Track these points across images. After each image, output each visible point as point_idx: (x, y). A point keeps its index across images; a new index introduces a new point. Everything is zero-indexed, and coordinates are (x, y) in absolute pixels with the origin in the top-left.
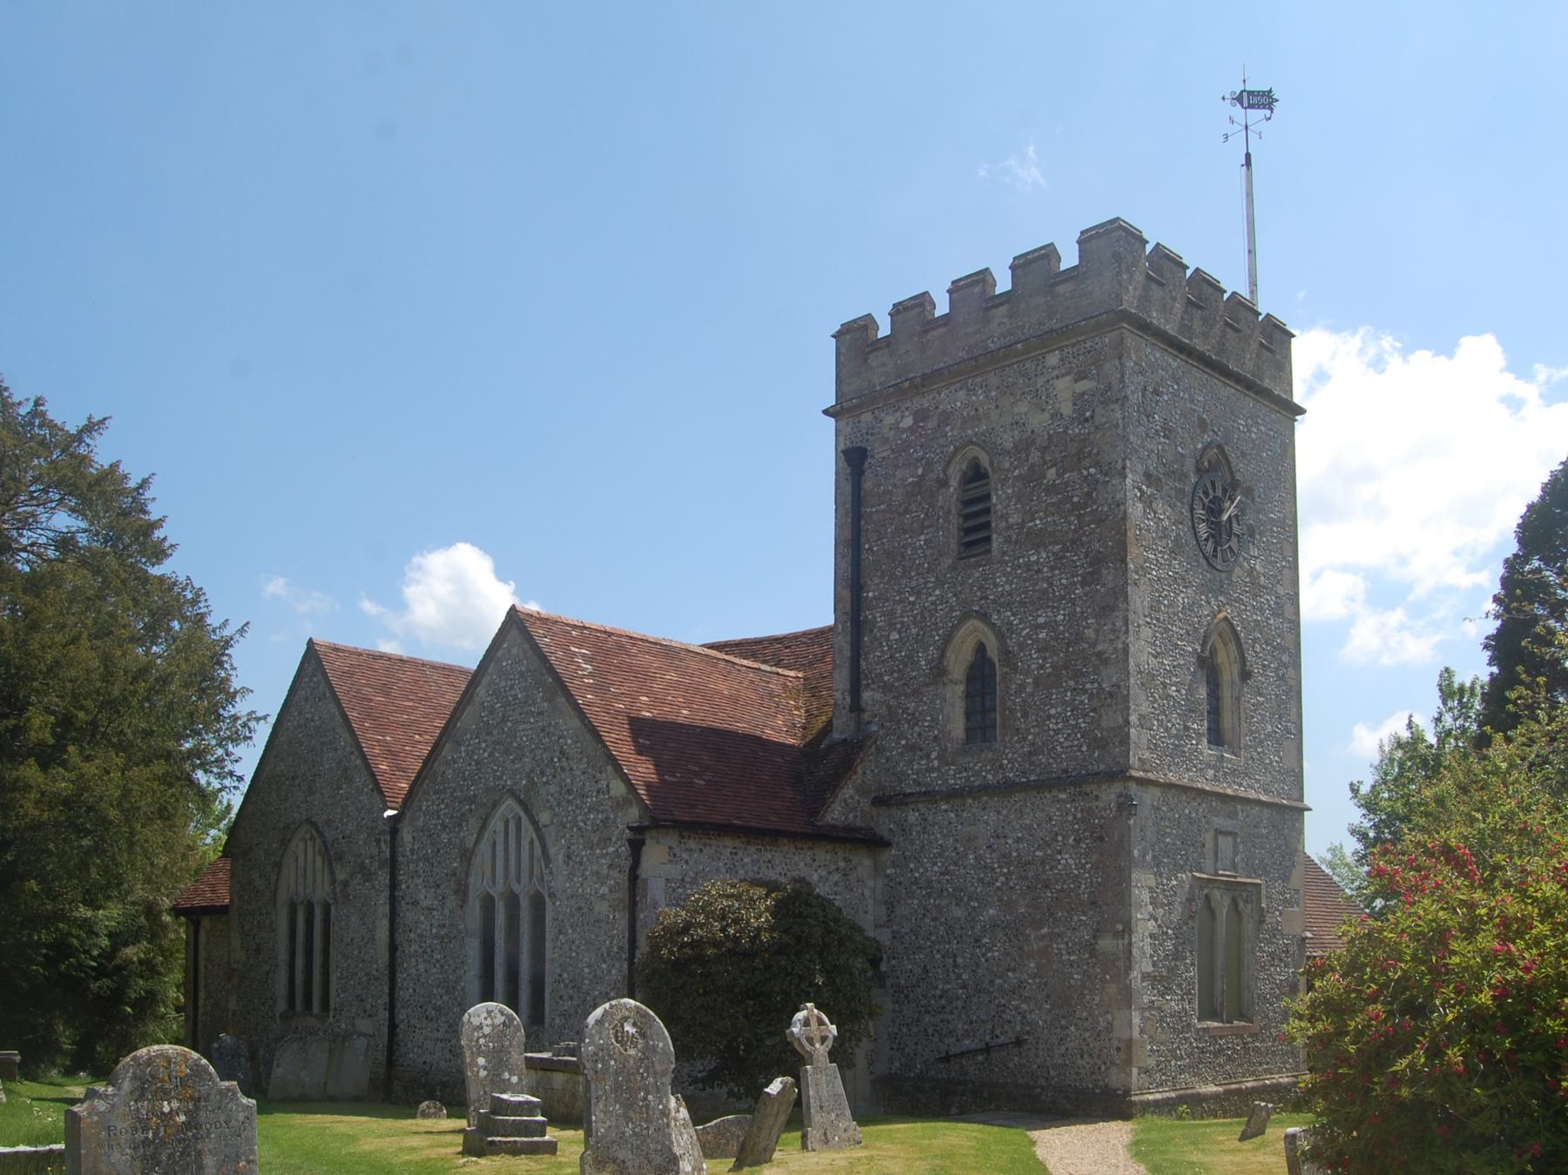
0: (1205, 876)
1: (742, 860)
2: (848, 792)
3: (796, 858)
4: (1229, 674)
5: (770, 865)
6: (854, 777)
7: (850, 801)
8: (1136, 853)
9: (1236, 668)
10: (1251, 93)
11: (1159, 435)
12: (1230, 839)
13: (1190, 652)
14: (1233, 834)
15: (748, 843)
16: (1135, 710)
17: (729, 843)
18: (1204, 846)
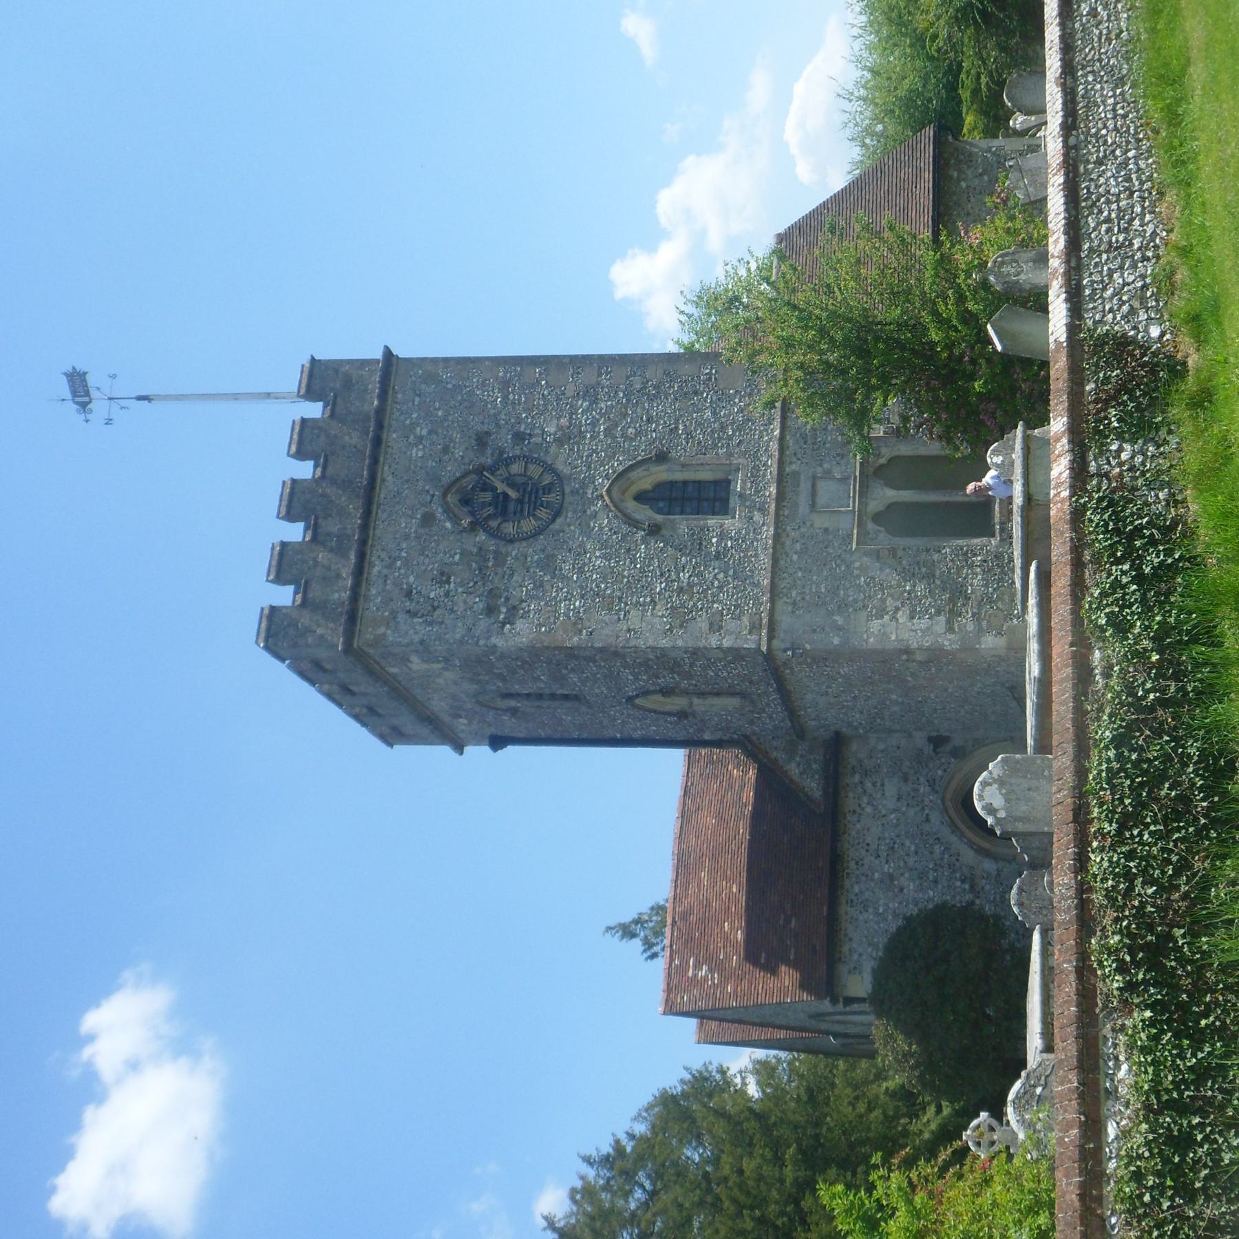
0: (855, 532)
1: (857, 895)
2: (793, 769)
3: (853, 833)
4: (661, 474)
5: (860, 863)
6: (780, 762)
7: (801, 768)
8: (836, 641)
9: (655, 469)
10: (75, 393)
11: (448, 591)
12: (821, 485)
13: (646, 547)
14: (814, 479)
15: (842, 887)
16: (707, 639)
17: (844, 909)
18: (826, 530)
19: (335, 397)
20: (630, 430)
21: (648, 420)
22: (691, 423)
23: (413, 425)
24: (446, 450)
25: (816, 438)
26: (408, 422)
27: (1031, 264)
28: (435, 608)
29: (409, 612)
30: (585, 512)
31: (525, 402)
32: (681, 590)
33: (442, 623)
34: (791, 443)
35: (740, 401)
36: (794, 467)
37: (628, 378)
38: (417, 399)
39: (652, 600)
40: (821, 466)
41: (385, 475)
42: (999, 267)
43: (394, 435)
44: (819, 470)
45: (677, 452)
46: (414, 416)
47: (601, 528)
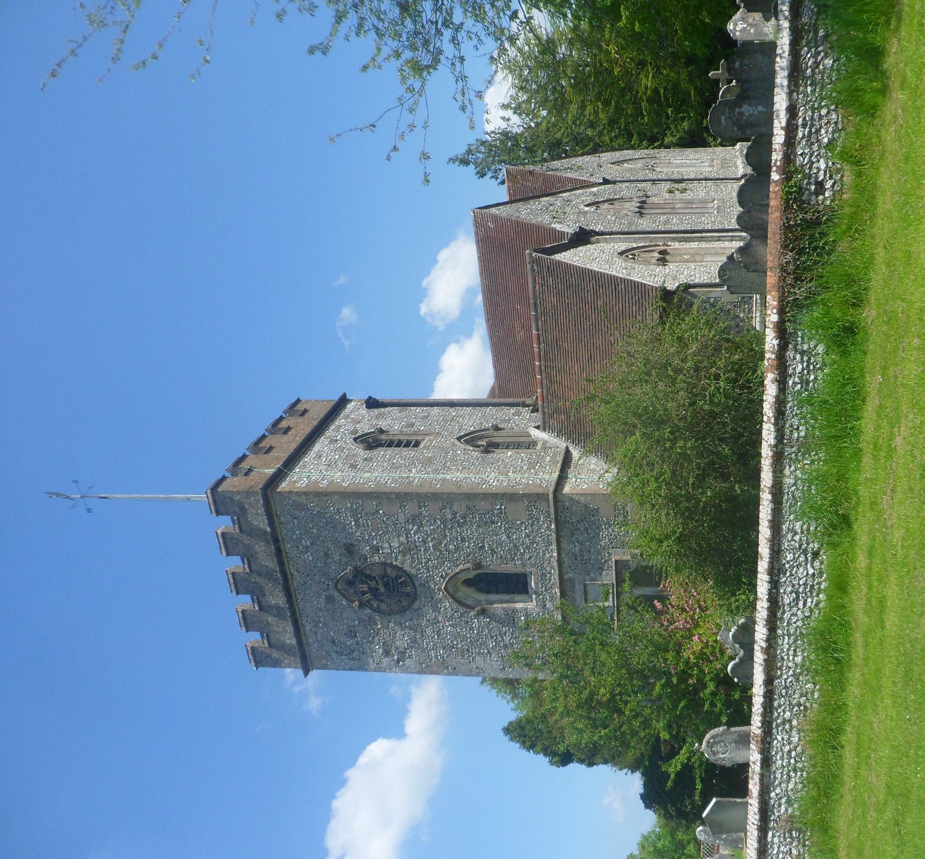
19: (238, 519)
20: (451, 546)
21: (462, 540)
22: (493, 543)
23: (299, 540)
24: (326, 555)
25: (583, 557)
26: (295, 537)
27: (733, 745)
28: (353, 651)
29: (336, 652)
30: (432, 598)
31: (372, 525)
32: (506, 646)
33: (359, 659)
34: (566, 559)
35: (526, 529)
36: (570, 575)
37: (441, 510)
38: (295, 521)
39: (488, 652)
40: (588, 575)
41: (292, 572)
42: (712, 747)
43: (289, 546)
44: (588, 578)
45: (487, 562)
46: (298, 532)
47: (446, 609)
